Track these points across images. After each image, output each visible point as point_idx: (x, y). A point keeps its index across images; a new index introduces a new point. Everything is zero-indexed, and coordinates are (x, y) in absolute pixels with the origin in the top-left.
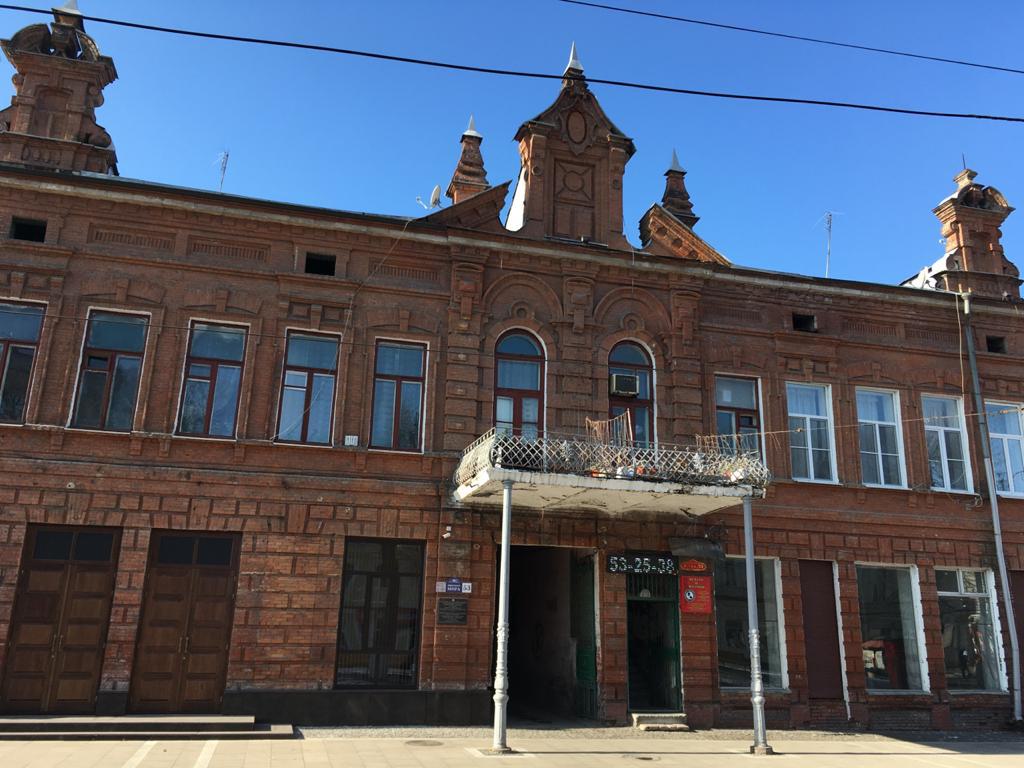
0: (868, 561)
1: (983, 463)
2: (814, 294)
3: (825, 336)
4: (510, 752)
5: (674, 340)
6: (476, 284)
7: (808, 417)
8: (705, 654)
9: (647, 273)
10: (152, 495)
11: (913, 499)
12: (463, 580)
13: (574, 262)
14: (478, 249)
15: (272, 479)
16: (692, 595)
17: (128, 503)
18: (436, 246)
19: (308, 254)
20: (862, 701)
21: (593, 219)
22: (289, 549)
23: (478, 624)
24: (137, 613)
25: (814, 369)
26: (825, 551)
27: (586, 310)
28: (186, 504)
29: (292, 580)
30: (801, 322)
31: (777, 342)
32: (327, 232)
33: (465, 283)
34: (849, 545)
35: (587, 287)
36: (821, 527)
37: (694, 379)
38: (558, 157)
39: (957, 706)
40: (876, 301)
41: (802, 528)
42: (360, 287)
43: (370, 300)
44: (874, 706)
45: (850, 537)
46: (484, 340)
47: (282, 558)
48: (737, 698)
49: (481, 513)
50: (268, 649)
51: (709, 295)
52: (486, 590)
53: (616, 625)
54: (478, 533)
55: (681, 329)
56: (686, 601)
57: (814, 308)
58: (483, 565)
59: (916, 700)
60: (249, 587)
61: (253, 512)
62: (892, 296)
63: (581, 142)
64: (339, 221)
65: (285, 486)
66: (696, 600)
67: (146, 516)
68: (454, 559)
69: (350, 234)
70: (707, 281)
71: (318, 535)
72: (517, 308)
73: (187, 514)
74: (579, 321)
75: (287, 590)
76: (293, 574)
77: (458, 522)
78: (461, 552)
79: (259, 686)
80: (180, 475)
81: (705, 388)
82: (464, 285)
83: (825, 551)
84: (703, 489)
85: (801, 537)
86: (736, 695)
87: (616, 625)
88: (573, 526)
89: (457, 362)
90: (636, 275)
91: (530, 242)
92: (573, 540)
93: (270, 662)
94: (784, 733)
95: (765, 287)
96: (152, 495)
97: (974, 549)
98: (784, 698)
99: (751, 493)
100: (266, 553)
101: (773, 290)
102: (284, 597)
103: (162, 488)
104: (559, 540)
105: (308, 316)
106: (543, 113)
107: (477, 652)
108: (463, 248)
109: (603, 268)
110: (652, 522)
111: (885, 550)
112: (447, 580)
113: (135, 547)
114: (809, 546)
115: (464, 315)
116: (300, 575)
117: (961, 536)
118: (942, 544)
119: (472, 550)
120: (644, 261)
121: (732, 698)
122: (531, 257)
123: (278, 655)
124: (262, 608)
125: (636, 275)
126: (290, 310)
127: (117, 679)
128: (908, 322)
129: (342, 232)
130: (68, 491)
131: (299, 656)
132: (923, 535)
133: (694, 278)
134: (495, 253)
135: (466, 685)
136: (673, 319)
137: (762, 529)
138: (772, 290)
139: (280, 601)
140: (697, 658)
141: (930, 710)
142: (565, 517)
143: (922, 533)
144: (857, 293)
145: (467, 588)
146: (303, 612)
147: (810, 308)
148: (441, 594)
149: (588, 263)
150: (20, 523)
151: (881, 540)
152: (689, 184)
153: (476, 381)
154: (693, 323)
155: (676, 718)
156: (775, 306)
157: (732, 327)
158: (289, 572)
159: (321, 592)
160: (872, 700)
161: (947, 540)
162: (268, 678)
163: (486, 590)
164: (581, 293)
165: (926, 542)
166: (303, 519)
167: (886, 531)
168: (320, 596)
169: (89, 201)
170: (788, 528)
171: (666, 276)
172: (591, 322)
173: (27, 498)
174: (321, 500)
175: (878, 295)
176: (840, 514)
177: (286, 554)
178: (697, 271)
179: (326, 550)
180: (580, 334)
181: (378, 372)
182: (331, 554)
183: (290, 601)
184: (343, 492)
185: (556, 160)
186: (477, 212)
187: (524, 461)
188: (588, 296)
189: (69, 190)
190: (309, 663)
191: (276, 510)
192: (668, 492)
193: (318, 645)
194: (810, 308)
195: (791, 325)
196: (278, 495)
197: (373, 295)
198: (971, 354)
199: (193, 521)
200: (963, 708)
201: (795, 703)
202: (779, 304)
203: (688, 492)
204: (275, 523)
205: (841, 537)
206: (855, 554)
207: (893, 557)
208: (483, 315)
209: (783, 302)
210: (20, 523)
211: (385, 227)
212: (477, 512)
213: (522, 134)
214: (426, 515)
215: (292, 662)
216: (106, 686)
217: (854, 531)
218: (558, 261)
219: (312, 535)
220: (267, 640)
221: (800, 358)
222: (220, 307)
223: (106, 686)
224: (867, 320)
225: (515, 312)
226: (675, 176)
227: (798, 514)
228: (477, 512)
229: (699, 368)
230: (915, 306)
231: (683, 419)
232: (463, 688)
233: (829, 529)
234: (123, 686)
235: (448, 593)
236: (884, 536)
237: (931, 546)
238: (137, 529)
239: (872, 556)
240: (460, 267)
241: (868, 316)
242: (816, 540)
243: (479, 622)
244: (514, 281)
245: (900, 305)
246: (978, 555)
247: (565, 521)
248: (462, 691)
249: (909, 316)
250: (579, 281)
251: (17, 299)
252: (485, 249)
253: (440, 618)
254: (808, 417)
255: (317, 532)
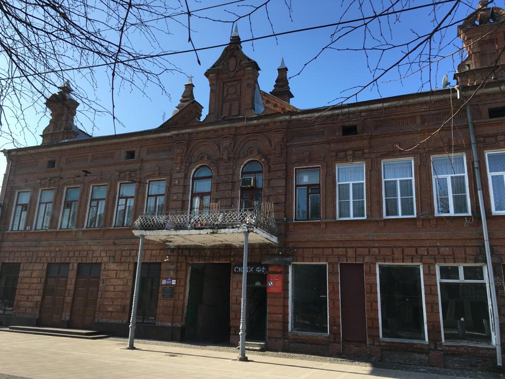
0: (385, 262)
1: (477, 192)
2: (354, 113)
3: (362, 135)
4: (134, 348)
5: (272, 155)
6: (183, 149)
7: (351, 183)
8: (280, 314)
9: (256, 126)
10: (77, 251)
11: (419, 223)
12: (172, 279)
13: (223, 129)
14: (183, 134)
15: (111, 242)
16: (272, 283)
17: (71, 254)
18: (169, 137)
19: (489, 109)
20: (376, 344)
21: (240, 106)
22: (115, 269)
23: (178, 298)
24: (72, 293)
25: (41, 183)
26: (356, 258)
27: (228, 150)
28: (86, 253)
29: (116, 280)
30: (349, 131)
31: (332, 145)
32: (131, 141)
33: (178, 150)
34: (372, 253)
35: (229, 139)
36: (354, 244)
37: (281, 174)
38: (224, 81)
39: (449, 353)
40: (396, 107)
41: (342, 245)
42: (142, 161)
43: (147, 165)
44: (384, 348)
45: (374, 249)
46: (187, 173)
47: (113, 272)
48: (297, 337)
49: (182, 249)
50: (107, 306)
51: (293, 128)
52: (182, 283)
53: (237, 299)
54: (180, 258)
55: (275, 149)
56: (269, 287)
57: (355, 121)
58: (182, 272)
59: (415, 346)
60: (103, 283)
61: (105, 255)
62: (404, 101)
63: (233, 71)
64: (133, 136)
65: (115, 244)
66: (274, 285)
67: (75, 258)
68: (169, 270)
69: (138, 140)
70: (289, 121)
71: (125, 262)
72: (200, 156)
73: (86, 257)
74: (225, 157)
75: (114, 284)
76: (116, 278)
77: (172, 254)
78: (172, 267)
79: (104, 320)
80: (85, 243)
81: (287, 178)
82: (178, 151)
83: (356, 258)
84: (223, 231)
85: (341, 251)
86: (297, 335)
87: (237, 299)
88: (220, 253)
89: (175, 185)
90: (253, 128)
91: (211, 124)
92: (219, 259)
93: (108, 312)
94: (147, 341)
95: (323, 117)
96: (77, 251)
97: (469, 251)
98: (325, 339)
99: (247, 230)
100: (108, 270)
101: (328, 117)
102: (113, 287)
103: (80, 248)
104: (213, 259)
105: (125, 177)
106: (216, 63)
107: (177, 310)
108: (177, 135)
109: (236, 128)
110: (257, 248)
111: (398, 254)
112: (166, 279)
113: (73, 270)
114: (346, 255)
115: (178, 164)
116: (118, 278)
117: (460, 244)
118: (442, 250)
119: (177, 266)
120: (254, 120)
121: (295, 337)
122: (206, 132)
123: (110, 309)
124: (106, 291)
125: (253, 128)
126: (120, 175)
127: (66, 316)
128: (423, 113)
129: (134, 141)
130: (57, 251)
131: (116, 309)
132: (428, 245)
133: (281, 122)
134: (190, 134)
135: (172, 324)
136: (272, 144)
137: (318, 248)
138: (328, 117)
139: (112, 288)
140: (275, 315)
141: (427, 353)
142: (216, 249)
143: (427, 243)
144: (380, 105)
145: (174, 282)
146: (119, 293)
147: (352, 121)
148: (164, 285)
149: (229, 128)
150: (45, 263)
151: (395, 250)
152: (195, 90)
153: (182, 192)
154: (281, 145)
155: (258, 344)
156: (332, 125)
157: (304, 142)
158: (115, 277)
159: (124, 285)
160: (384, 344)
161: (446, 247)
162: (106, 318)
163: (182, 283)
164: (226, 143)
165: (430, 249)
166: (120, 256)
167: (399, 244)
168: (124, 286)
169: (65, 150)
170: (333, 246)
171: (267, 124)
172: (232, 155)
173: (47, 255)
174: (126, 248)
175: (394, 103)
176: (366, 236)
177: (115, 270)
178: (281, 118)
179: (127, 268)
180: (227, 162)
181: (19, 203)
182: (128, 270)
183: (115, 289)
184: (133, 245)
185: (224, 83)
186: (184, 118)
187: (146, 226)
188: (230, 143)
189: (58, 148)
190: (120, 312)
191: (112, 253)
192: (207, 233)
193: (123, 305)
194: (352, 121)
195: (341, 133)
196: (112, 248)
197: (147, 163)
198: (470, 124)
199: (88, 259)
200: (453, 354)
201: (332, 342)
202: (334, 123)
203: (216, 233)
204: (111, 258)
205: (367, 249)
206: (376, 258)
207: (466, 259)
208: (186, 162)
209: (335, 122)
210: (45, 263)
211: (147, 135)
212: (180, 249)
213: (207, 74)
214: (162, 252)
215: (114, 312)
216: (63, 318)
217: (376, 245)
218: (215, 131)
219: (123, 262)
220: (107, 303)
221: (345, 151)
222: (99, 180)
223: (63, 318)
224: (393, 119)
225: (199, 158)
226: (283, 71)
227: (339, 238)
228: (180, 249)
229: (285, 167)
230: (426, 103)
231: (274, 195)
232: (170, 325)
233: (359, 245)
234: (68, 318)
235: (167, 285)
236: (398, 247)
237: (433, 252)
238: (73, 263)
239: (388, 259)
240: (178, 143)
241: (393, 117)
242: (350, 252)
243: (179, 297)
244: (200, 144)
245: (414, 105)
246: (474, 255)
247: (216, 250)
248: (170, 326)
249: (423, 110)
250: (226, 137)
251: (47, 188)
252: (186, 133)
253: (163, 295)
254: (351, 183)
255: (124, 261)
